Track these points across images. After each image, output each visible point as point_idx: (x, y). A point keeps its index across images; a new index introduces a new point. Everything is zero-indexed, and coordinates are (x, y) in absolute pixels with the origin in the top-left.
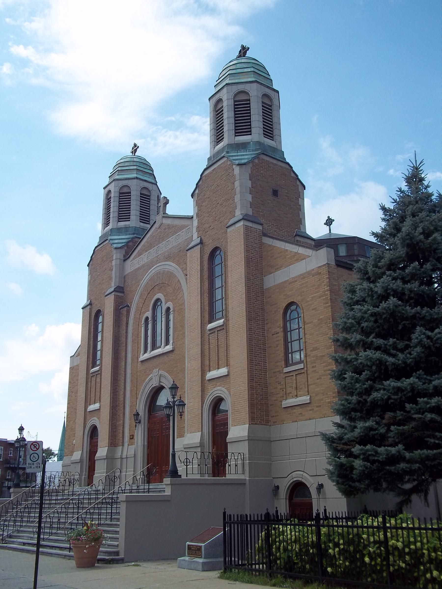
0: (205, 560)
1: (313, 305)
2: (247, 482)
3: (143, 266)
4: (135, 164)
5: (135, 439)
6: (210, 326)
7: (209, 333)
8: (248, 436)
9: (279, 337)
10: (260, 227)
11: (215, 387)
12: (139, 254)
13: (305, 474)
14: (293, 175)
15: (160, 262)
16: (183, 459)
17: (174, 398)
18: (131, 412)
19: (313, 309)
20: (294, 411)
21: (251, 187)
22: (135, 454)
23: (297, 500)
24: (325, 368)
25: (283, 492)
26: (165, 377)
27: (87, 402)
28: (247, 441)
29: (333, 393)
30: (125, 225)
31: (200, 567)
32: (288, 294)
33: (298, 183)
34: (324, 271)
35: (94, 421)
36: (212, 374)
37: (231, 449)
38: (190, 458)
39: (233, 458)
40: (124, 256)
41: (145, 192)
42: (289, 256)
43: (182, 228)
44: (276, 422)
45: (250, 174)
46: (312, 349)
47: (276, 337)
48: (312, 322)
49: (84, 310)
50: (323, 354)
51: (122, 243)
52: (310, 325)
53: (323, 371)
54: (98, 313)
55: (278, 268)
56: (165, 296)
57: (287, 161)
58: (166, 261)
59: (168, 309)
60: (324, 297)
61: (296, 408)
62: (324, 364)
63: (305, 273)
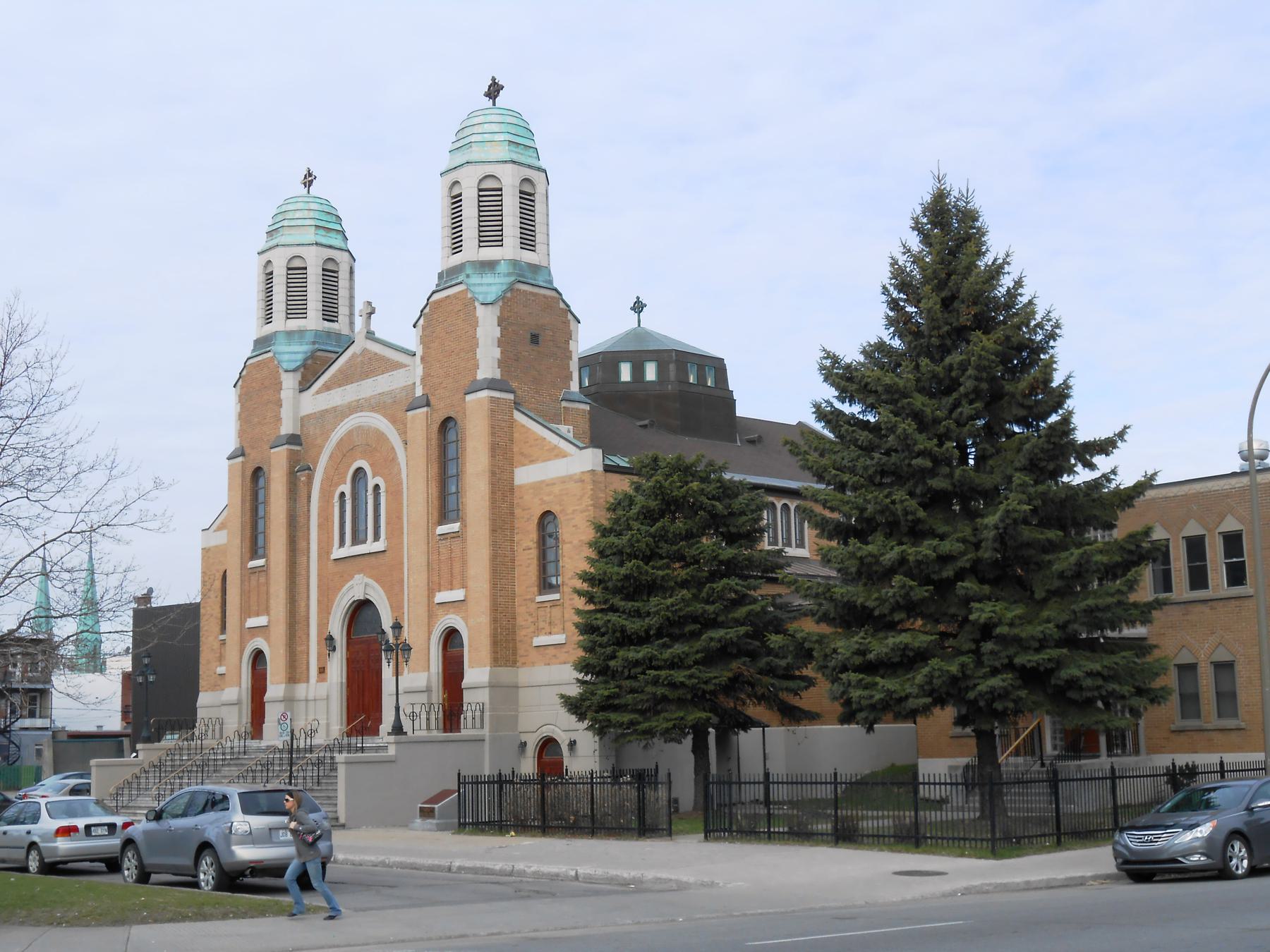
0: (438, 821)
2: (487, 739)
3: (335, 409)
4: (312, 214)
7: (438, 538)
8: (489, 683)
10: (511, 396)
12: (327, 387)
13: (556, 729)
14: (562, 305)
16: (409, 710)
17: (397, 639)
18: (319, 636)
20: (547, 651)
21: (499, 336)
22: (328, 696)
23: (546, 758)
25: (531, 750)
26: (373, 588)
28: (487, 690)
31: (434, 827)
33: (570, 317)
34: (587, 478)
35: (259, 643)
36: (441, 597)
37: (468, 697)
38: (417, 710)
39: (469, 708)
40: (300, 383)
41: (330, 266)
43: (398, 366)
45: (498, 317)
51: (296, 361)
54: (257, 472)
56: (371, 465)
57: (556, 285)
59: (377, 487)
61: (550, 647)
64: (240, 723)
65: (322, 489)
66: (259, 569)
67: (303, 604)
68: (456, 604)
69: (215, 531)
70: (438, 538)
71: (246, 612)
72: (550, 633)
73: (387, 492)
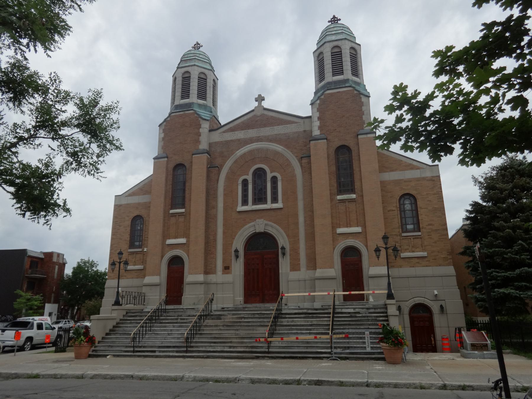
3: (239, 140)
5: (231, 270)
6: (339, 197)
7: (337, 201)
11: (347, 239)
19: (428, 201)
20: (411, 260)
25: (406, 310)
26: (272, 227)
32: (404, 188)
36: (340, 230)
44: (394, 266)
46: (427, 224)
49: (156, 160)
62: (439, 235)
63: (420, 178)
64: (160, 296)
65: (228, 178)
68: (354, 234)
69: (126, 196)
70: (337, 201)
71: (166, 236)
72: (414, 251)
73: (282, 180)
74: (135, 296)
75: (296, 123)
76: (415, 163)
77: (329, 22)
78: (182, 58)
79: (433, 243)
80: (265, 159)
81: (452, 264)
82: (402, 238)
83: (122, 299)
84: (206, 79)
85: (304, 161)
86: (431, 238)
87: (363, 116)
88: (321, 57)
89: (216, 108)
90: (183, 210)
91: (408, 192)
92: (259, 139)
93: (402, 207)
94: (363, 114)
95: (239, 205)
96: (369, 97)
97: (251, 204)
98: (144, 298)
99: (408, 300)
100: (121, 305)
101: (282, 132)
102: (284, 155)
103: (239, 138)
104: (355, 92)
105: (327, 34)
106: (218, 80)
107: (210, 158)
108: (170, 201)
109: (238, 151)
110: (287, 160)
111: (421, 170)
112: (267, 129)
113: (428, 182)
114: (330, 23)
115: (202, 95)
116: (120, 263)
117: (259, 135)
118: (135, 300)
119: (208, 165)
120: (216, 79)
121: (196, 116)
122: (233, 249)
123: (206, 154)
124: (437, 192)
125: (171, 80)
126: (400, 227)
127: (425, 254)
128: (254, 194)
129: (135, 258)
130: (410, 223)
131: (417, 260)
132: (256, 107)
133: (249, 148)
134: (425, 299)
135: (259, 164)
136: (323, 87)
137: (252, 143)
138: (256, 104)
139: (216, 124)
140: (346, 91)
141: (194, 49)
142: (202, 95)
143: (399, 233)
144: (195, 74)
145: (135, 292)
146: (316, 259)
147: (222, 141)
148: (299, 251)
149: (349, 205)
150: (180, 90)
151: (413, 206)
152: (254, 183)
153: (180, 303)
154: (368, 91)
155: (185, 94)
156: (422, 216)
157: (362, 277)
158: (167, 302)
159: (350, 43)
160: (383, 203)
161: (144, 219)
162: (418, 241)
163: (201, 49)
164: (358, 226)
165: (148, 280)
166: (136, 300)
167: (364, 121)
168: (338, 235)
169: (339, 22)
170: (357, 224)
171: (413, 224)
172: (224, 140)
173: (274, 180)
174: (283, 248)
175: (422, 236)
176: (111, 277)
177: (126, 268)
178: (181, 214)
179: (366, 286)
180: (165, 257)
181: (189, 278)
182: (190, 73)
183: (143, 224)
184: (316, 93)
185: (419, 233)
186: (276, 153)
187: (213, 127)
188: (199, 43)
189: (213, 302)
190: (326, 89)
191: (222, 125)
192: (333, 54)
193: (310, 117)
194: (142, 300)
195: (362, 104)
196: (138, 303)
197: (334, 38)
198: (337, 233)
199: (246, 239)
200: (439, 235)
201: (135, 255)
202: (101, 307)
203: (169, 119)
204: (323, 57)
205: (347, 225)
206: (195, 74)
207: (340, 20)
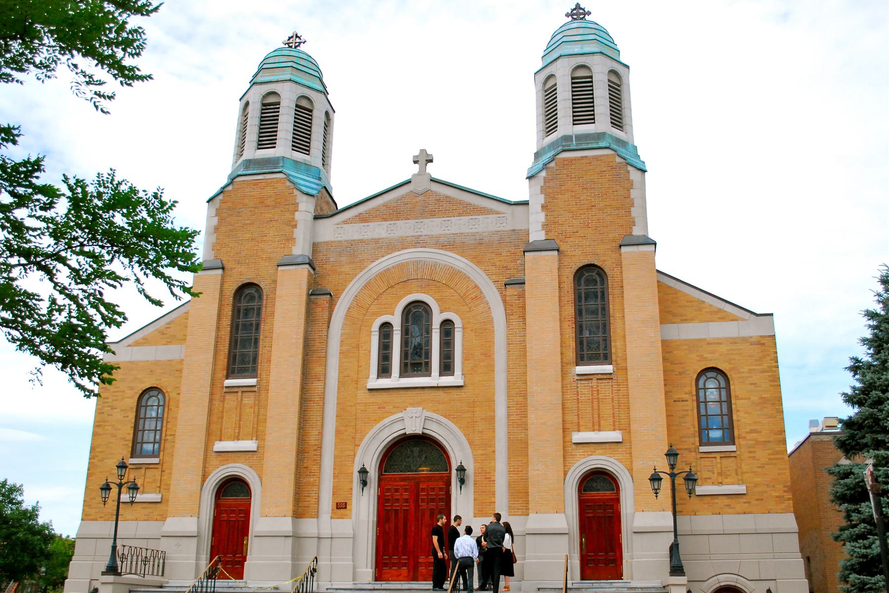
1: (750, 379)
3: (376, 241)
5: (351, 510)
7: (577, 378)
9: (687, 405)
11: (592, 455)
15: (425, 247)
19: (751, 384)
20: (716, 501)
24: (772, 457)
26: (439, 423)
27: (210, 436)
29: (784, 487)
30: (305, 160)
32: (706, 355)
36: (577, 437)
42: (708, 310)
46: (748, 430)
47: (682, 406)
48: (749, 399)
50: (768, 440)
52: (746, 401)
53: (767, 460)
55: (686, 320)
56: (437, 300)
58: (441, 249)
60: (770, 374)
61: (720, 497)
66: (245, 389)
67: (314, 432)
69: (130, 346)
70: (577, 378)
72: (721, 483)
73: (464, 328)
74: (146, 557)
75: (497, 213)
76: (728, 308)
77: (567, 15)
78: (263, 63)
79: (758, 467)
80: (430, 283)
81: (792, 509)
82: (700, 455)
83: (122, 562)
84: (311, 111)
85: (512, 291)
86: (753, 458)
87: (632, 209)
88: (550, 83)
89: (328, 172)
90: (252, 381)
91: (714, 366)
92: (418, 242)
93: (701, 393)
94: (632, 205)
95: (371, 376)
96: (644, 171)
97: (398, 375)
98: (164, 563)
99: (705, 579)
100: (120, 574)
101: (465, 230)
102: (469, 278)
103: (376, 236)
104: (618, 160)
105: (564, 39)
106: (334, 112)
107: (315, 274)
108: (226, 360)
109: (375, 264)
110: (476, 287)
111: (739, 322)
112: (437, 221)
113: (752, 346)
114: (570, 19)
115: (302, 142)
116: (120, 486)
117: (419, 234)
118: (145, 565)
119: (309, 289)
120: (331, 111)
121: (289, 186)
122: (357, 468)
123: (307, 266)
124: (768, 367)
125: (237, 107)
126: (697, 434)
127: (742, 489)
128: (404, 355)
129: (143, 478)
130: (715, 427)
131: (726, 501)
132: (414, 175)
133: (397, 259)
134: (739, 577)
135: (418, 292)
136: (552, 145)
137: (402, 249)
138: (416, 168)
139: (328, 203)
140: (601, 156)
141: (287, 46)
142: (302, 142)
143: (693, 446)
144: (288, 98)
145: (147, 549)
146: (527, 493)
147: (340, 242)
148: (494, 476)
149: (598, 386)
150: (256, 130)
151: (724, 392)
152: (405, 332)
153: (239, 575)
154: (642, 159)
155: (267, 138)
156: (739, 413)
157: (620, 532)
158: (212, 574)
159: (608, 61)
160: (665, 385)
161: (166, 395)
162: (730, 463)
163: (303, 48)
164: (614, 430)
165: (175, 524)
166: (147, 566)
167: (634, 218)
168: (574, 446)
169: (587, 17)
170: (614, 425)
171: (721, 428)
172: (346, 238)
173: (447, 326)
174: (461, 469)
175: (738, 453)
176: (90, 515)
177: (133, 497)
178: (249, 389)
179: (626, 551)
180: (210, 477)
181: (259, 524)
182: (279, 95)
183: (164, 406)
184: (537, 155)
185: (732, 448)
186: (455, 274)
187: (321, 209)
188: (299, 35)
189: (315, 574)
190: (560, 148)
191: (340, 207)
192: (575, 82)
193: (525, 203)
194: (158, 566)
195: (630, 185)
196: (150, 573)
197: (577, 49)
198: (573, 442)
199: (385, 447)
200: (770, 452)
201: (143, 471)
202: (66, 578)
203: (230, 188)
204: (555, 85)
205: (593, 426)
206: (288, 98)
207: (589, 13)
